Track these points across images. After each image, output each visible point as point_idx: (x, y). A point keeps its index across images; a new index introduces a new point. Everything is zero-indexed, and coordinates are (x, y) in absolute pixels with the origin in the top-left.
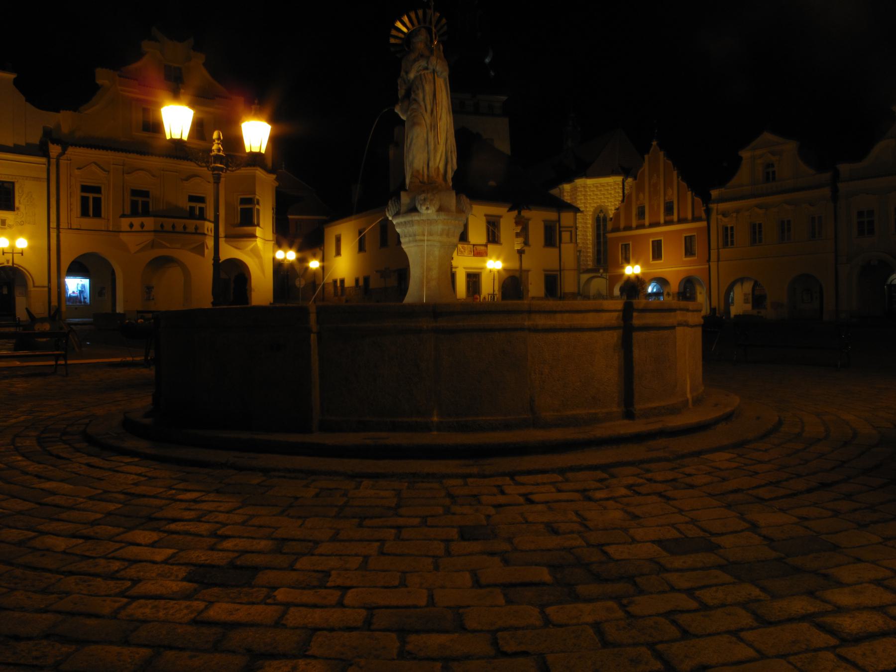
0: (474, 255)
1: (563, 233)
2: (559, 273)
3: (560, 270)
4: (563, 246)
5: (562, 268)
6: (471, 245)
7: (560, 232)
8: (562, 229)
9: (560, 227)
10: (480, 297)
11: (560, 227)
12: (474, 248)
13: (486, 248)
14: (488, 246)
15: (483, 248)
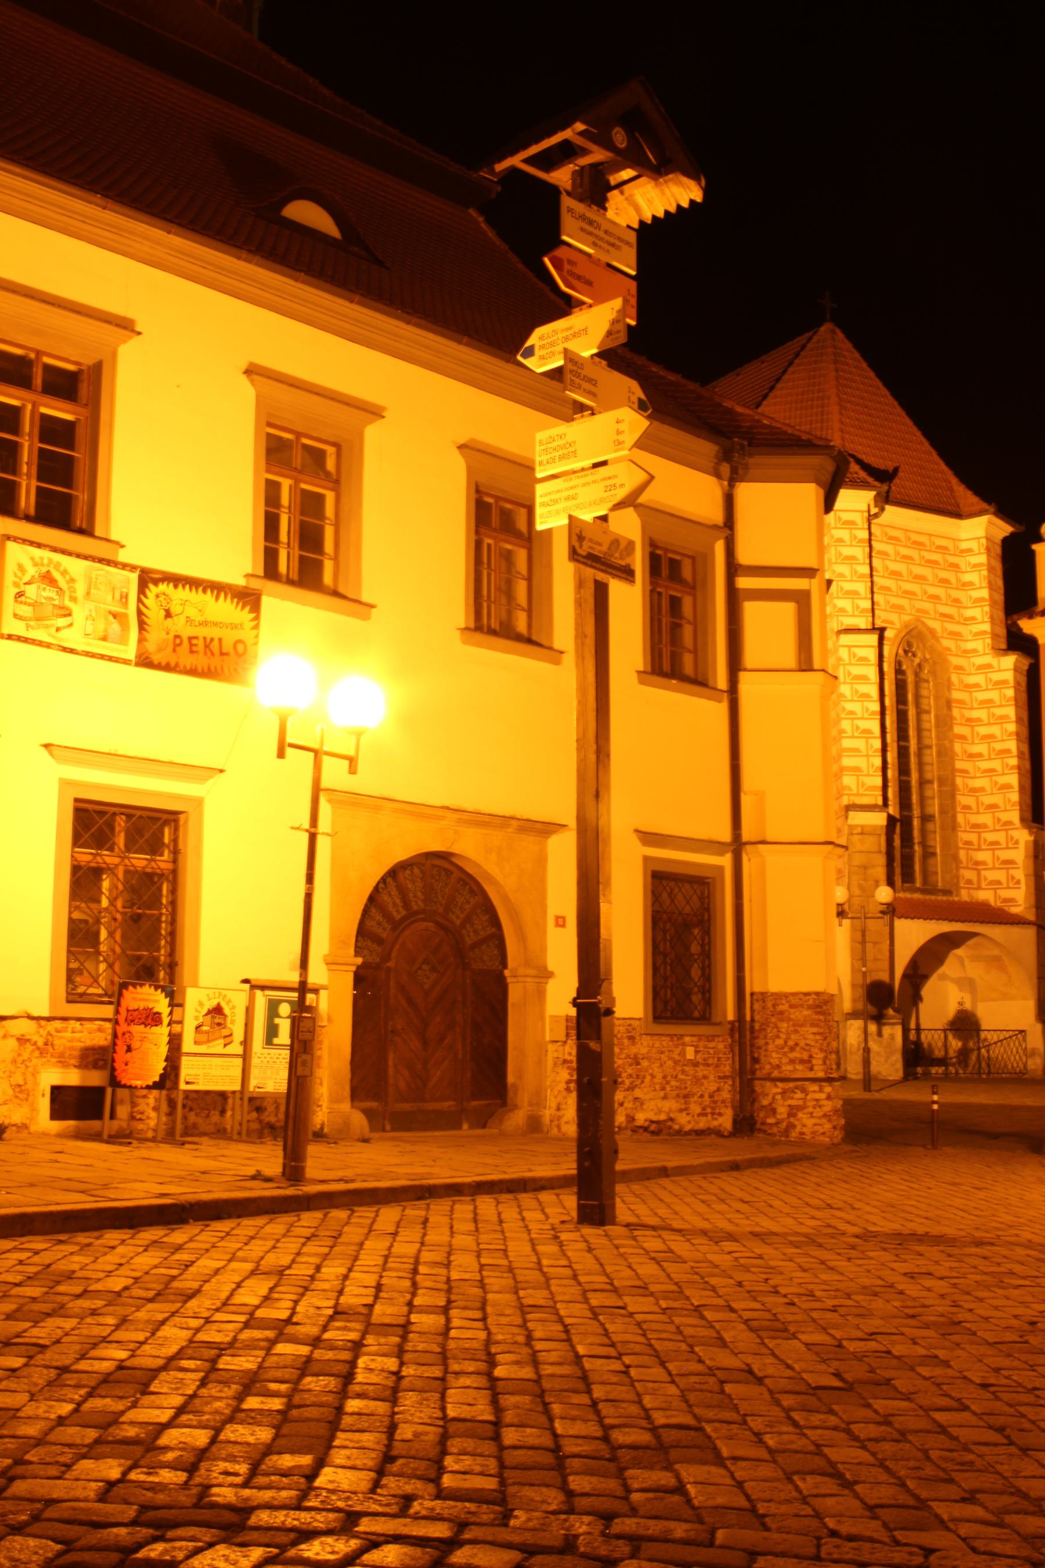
0: (145, 661)
1: (751, 610)
2: (726, 861)
3: (737, 846)
4: (747, 683)
5: (746, 835)
6: (133, 568)
7: (734, 599)
8: (744, 582)
9: (733, 569)
10: (176, 1002)
11: (733, 569)
12: (150, 601)
13: (244, 616)
14: (267, 602)
15: (225, 610)
